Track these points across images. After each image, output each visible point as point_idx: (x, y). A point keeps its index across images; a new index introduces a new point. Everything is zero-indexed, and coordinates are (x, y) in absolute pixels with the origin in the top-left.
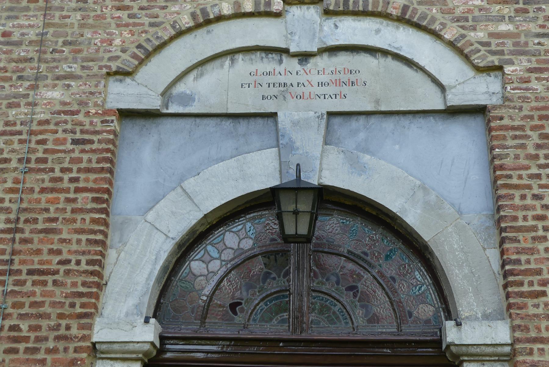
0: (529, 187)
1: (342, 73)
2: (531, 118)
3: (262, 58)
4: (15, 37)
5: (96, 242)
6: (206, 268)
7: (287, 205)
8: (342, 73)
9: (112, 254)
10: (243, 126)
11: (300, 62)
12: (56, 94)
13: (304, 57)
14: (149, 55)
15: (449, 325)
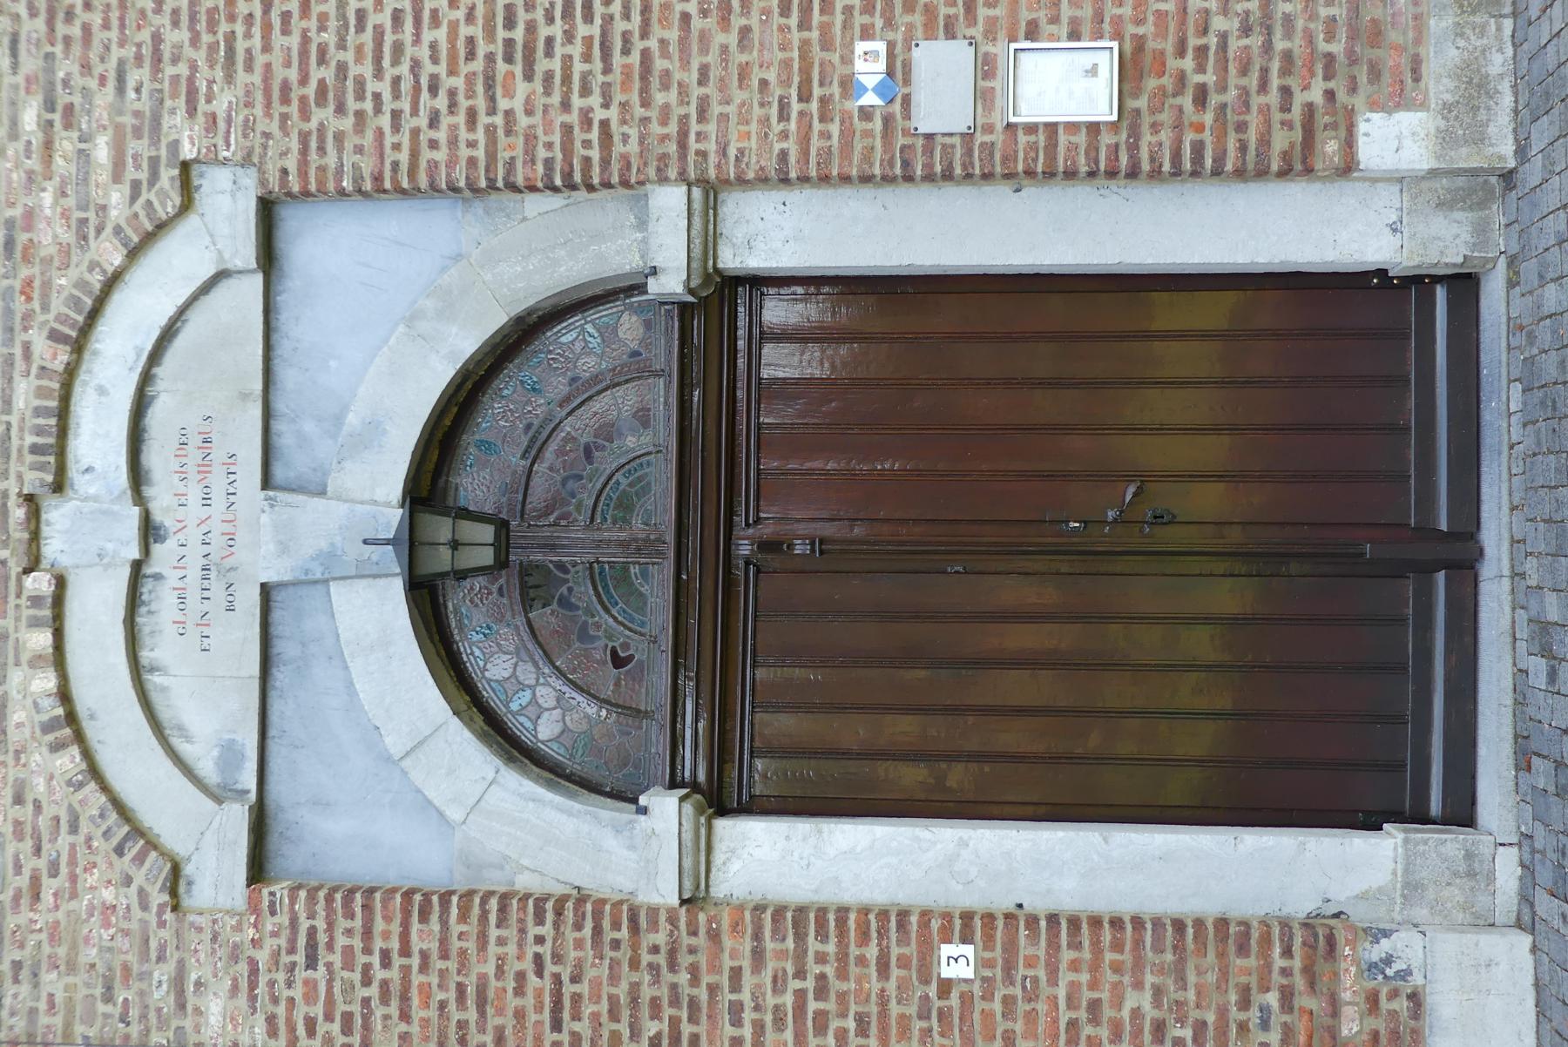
0: (415, 133)
1: (184, 460)
2: (284, 118)
3: (149, 612)
5: (503, 909)
6: (548, 711)
7: (441, 560)
8: (184, 460)
9: (525, 882)
10: (284, 648)
11: (160, 539)
12: (215, 1008)
13: (149, 531)
14: (138, 831)
15: (654, 286)
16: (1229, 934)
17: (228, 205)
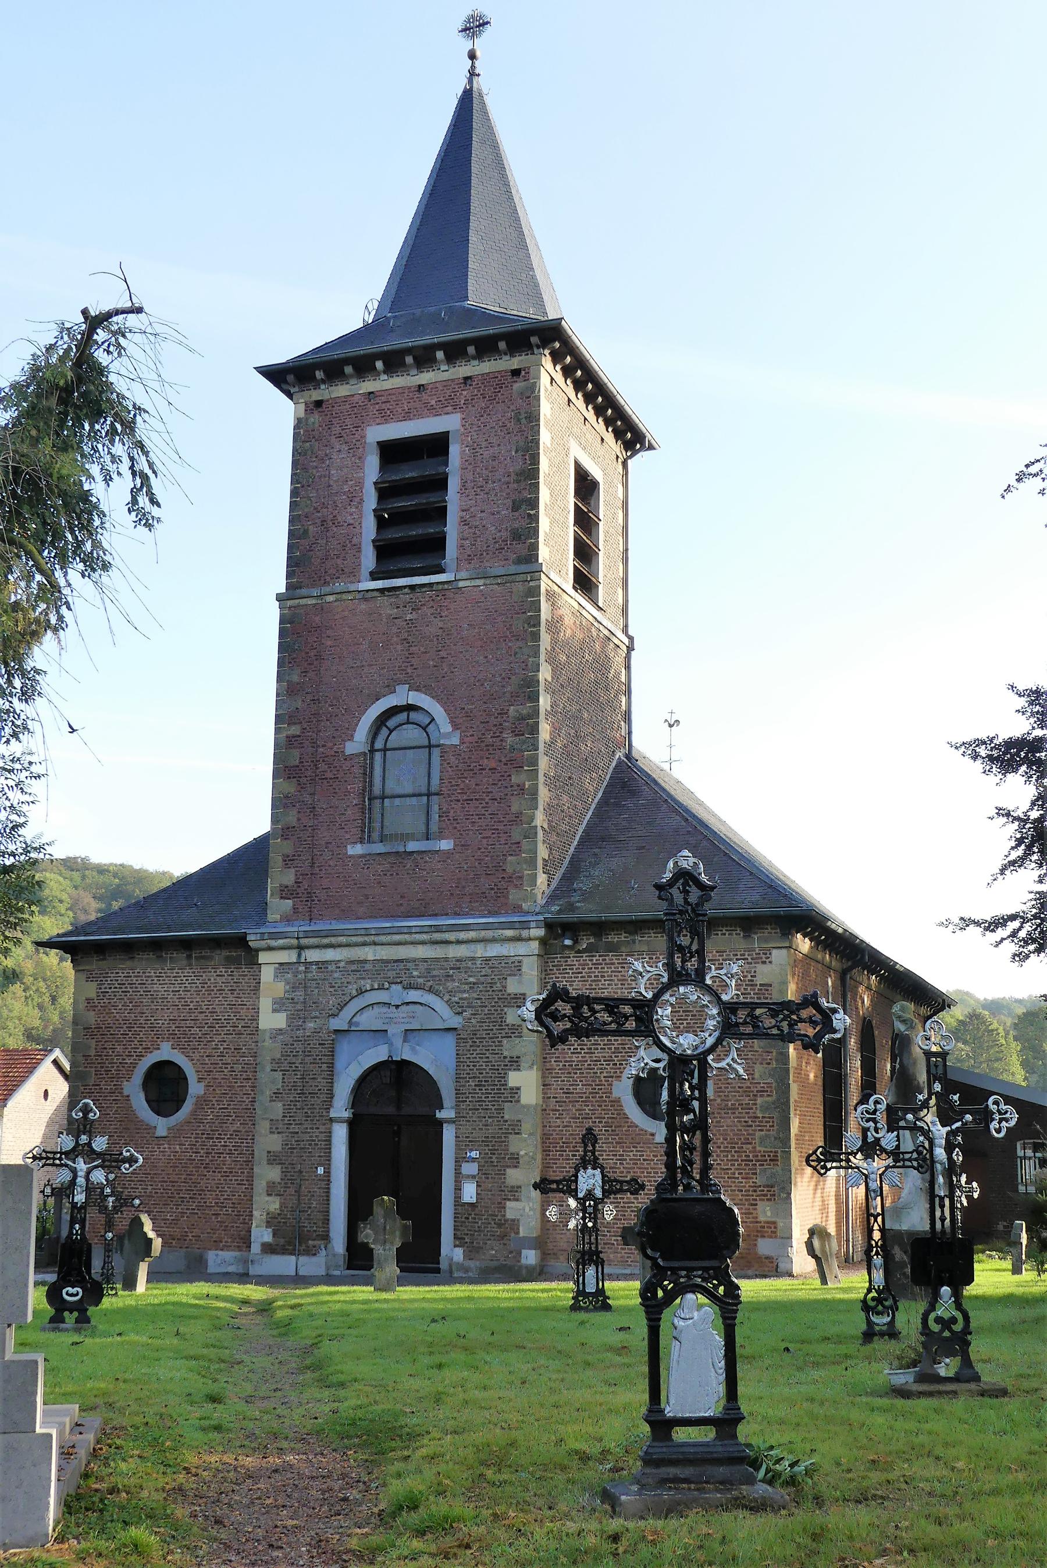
4: (296, 1000)
9: (335, 1084)
10: (377, 1034)
12: (312, 1025)
13: (397, 1007)
14: (342, 1008)
16: (327, 1221)
17: (456, 1022)
